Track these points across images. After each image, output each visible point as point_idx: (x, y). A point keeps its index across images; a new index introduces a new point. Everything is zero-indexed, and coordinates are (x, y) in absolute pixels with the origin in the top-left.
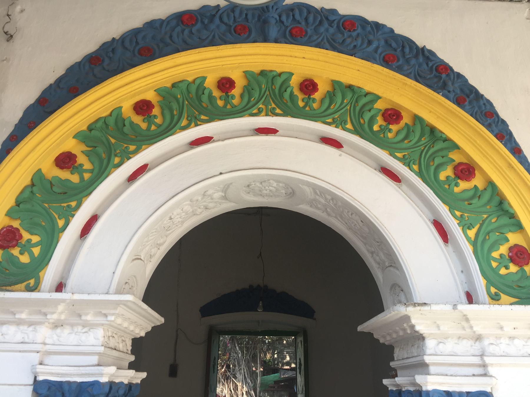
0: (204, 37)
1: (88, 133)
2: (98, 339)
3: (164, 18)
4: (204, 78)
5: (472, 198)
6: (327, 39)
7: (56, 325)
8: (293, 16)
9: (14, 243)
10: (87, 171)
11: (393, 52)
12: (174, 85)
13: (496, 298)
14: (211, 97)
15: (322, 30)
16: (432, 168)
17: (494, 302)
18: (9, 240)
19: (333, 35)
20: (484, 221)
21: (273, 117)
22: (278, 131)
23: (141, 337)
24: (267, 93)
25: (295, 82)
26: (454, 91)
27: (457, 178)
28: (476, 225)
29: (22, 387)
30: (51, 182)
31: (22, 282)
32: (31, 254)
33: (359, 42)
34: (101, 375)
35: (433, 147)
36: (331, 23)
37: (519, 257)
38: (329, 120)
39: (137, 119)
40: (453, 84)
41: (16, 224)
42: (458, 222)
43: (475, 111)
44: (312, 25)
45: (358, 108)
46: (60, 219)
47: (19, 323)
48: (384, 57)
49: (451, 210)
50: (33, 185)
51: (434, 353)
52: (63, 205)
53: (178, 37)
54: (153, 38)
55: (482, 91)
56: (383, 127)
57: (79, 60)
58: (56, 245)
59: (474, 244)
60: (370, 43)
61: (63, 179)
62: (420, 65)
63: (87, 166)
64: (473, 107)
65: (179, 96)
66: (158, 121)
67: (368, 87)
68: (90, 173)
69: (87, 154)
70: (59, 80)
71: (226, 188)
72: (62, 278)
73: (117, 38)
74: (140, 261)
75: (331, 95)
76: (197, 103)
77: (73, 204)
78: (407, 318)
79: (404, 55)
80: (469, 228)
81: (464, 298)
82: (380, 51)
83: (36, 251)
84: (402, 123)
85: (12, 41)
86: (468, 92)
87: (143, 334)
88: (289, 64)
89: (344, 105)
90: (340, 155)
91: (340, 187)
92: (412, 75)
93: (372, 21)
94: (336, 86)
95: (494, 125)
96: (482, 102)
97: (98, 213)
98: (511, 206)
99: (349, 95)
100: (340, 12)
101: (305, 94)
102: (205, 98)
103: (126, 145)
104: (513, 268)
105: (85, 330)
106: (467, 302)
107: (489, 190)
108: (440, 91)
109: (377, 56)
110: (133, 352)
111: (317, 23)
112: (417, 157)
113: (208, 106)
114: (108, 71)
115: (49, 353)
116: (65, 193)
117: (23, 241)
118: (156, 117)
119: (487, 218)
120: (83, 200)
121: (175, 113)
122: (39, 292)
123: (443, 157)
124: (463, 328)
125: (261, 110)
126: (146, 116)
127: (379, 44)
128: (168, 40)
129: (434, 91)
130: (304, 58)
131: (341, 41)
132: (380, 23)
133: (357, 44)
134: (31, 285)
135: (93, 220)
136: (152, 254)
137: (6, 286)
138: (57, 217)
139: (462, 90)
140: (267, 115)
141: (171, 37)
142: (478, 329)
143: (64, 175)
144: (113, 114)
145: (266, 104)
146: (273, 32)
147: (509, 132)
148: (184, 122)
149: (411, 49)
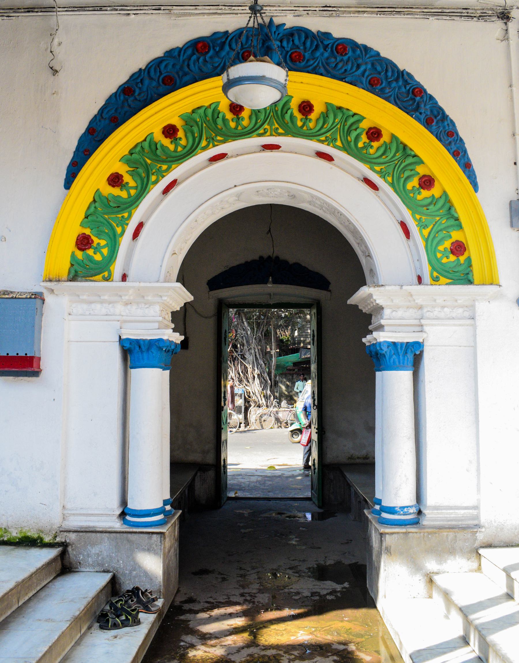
0: (216, 65)
1: (129, 157)
2: (156, 312)
3: (181, 46)
4: (218, 103)
5: (430, 204)
6: (322, 63)
7: (127, 304)
8: (293, 41)
9: (89, 245)
10: (132, 188)
11: (377, 76)
12: (193, 111)
13: (437, 279)
14: (224, 120)
15: (318, 54)
16: (402, 180)
17: (435, 283)
18: (85, 244)
19: (327, 59)
20: (436, 222)
21: (276, 136)
22: (280, 147)
24: (271, 114)
26: (425, 112)
27: (420, 188)
28: (429, 226)
29: (112, 343)
30: (107, 199)
31: (99, 274)
32: (102, 254)
33: (349, 66)
34: (164, 334)
35: (405, 162)
36: (326, 47)
37: (457, 250)
39: (166, 142)
40: (425, 105)
41: (88, 232)
42: (417, 223)
43: (440, 130)
44: (310, 48)
45: (346, 127)
46: (118, 227)
47: (102, 302)
48: (370, 80)
49: (413, 214)
50: (94, 201)
51: (389, 318)
52: (118, 216)
53: (194, 64)
54: (174, 65)
55: (448, 112)
56: (366, 144)
57: (114, 91)
58: (119, 247)
59: (427, 241)
60: (358, 67)
61: (116, 195)
62: (399, 88)
63: (132, 184)
64: (439, 126)
65: (198, 120)
66: (183, 142)
67: (354, 110)
68: (135, 189)
69: (131, 174)
70: (102, 111)
71: (239, 196)
72: (124, 270)
73: (143, 68)
75: (325, 116)
76: (213, 125)
77: (126, 215)
78: (370, 296)
79: (387, 78)
80: (424, 228)
81: (416, 280)
82: (367, 73)
83: (105, 251)
84: (382, 140)
85: (57, 74)
86: (436, 113)
89: (335, 124)
90: (331, 168)
92: (392, 98)
93: (361, 44)
94: (329, 108)
95: (453, 144)
96: (446, 123)
98: (456, 212)
99: (340, 116)
100: (333, 36)
101: (303, 115)
102: (220, 121)
103: (159, 165)
104: (452, 258)
105: (147, 306)
106: (417, 283)
107: (444, 198)
108: (412, 113)
109: (364, 80)
111: (314, 47)
112: (391, 171)
113: (222, 129)
114: (140, 101)
115: (125, 322)
116: (118, 207)
117: (95, 244)
118: (181, 140)
119: (439, 219)
120: (133, 211)
121: (196, 135)
122: (112, 281)
123: (412, 170)
124: (410, 301)
125: (266, 130)
126: (173, 139)
127: (366, 68)
128: (186, 69)
129: (408, 113)
130: (302, 83)
131: (334, 65)
132: (369, 46)
133: (348, 68)
134: (106, 276)
135: (141, 225)
139: (432, 111)
140: (271, 135)
141: (188, 65)
142: (419, 301)
143: (116, 191)
144: (147, 140)
145: (271, 124)
147: (464, 149)
148: (204, 143)
149: (393, 71)
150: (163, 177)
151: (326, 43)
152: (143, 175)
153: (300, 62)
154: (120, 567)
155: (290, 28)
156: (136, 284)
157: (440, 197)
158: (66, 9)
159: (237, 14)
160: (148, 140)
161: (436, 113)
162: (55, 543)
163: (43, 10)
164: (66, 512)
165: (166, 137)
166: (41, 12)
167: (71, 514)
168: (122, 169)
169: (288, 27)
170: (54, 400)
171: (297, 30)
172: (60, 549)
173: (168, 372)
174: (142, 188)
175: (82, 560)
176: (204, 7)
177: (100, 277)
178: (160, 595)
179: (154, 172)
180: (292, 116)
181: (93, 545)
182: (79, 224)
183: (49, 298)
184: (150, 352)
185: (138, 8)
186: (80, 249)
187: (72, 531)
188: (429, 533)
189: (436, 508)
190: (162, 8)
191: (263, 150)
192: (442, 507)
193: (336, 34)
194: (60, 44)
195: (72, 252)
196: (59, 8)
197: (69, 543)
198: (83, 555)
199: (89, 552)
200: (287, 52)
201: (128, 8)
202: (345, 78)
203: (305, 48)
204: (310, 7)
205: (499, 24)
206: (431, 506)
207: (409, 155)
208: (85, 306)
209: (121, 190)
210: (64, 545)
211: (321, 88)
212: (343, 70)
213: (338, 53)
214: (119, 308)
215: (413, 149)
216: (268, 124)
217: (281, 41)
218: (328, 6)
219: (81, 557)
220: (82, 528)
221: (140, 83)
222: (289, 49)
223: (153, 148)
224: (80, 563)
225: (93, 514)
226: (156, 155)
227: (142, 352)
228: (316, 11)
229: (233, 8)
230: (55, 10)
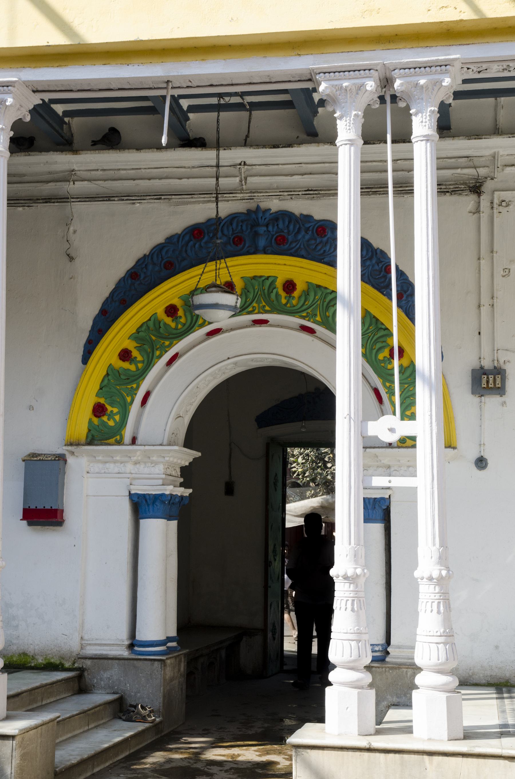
3: (180, 233)
7: (136, 463)
8: (277, 225)
9: (104, 412)
10: (139, 362)
13: (404, 441)
15: (300, 236)
16: (374, 351)
17: (402, 445)
23: (186, 466)
24: (259, 293)
25: (279, 284)
29: (124, 497)
31: (112, 438)
32: (114, 420)
34: (166, 490)
35: (377, 334)
38: (304, 314)
39: (168, 320)
41: (102, 401)
43: (409, 304)
45: (325, 304)
47: (115, 462)
50: (107, 374)
52: (128, 387)
54: (174, 251)
58: (129, 414)
61: (126, 368)
62: (373, 266)
63: (139, 358)
64: (409, 301)
66: (183, 320)
70: (112, 293)
72: (134, 433)
73: (147, 254)
74: (180, 418)
75: (306, 294)
77: (135, 386)
83: (117, 418)
87: (187, 464)
88: (273, 269)
89: (316, 301)
90: (313, 341)
91: (311, 366)
97: (150, 389)
99: (319, 294)
100: (315, 218)
101: (287, 293)
103: (162, 342)
105: (153, 465)
107: (411, 367)
108: (383, 290)
110: (182, 476)
115: (135, 479)
116: (128, 379)
119: (407, 387)
120: (140, 383)
124: (377, 461)
125: (254, 308)
128: (184, 255)
131: (314, 247)
134: (118, 440)
135: (147, 395)
136: (188, 410)
137: (104, 440)
138: (126, 395)
140: (259, 313)
141: (186, 251)
142: (386, 461)
143: (126, 365)
145: (259, 302)
146: (262, 242)
150: (166, 352)
151: (307, 225)
152: (149, 350)
153: (283, 245)
154: (127, 690)
155: (276, 212)
156: (142, 448)
157: (409, 367)
158: (79, 200)
159: (228, 201)
160: (152, 319)
161: (405, 289)
162: (74, 668)
163: (59, 200)
164: (83, 642)
165: (168, 316)
166: (57, 202)
167: (86, 644)
168: (130, 345)
169: (274, 212)
170: (75, 546)
171: (282, 214)
172: (78, 672)
173: (174, 524)
174: (148, 361)
175: (96, 683)
176: (199, 196)
177: (112, 440)
178: (160, 715)
179: (158, 348)
180: (277, 295)
181: (105, 670)
182: (95, 395)
183: (70, 460)
184: (155, 506)
185: (142, 198)
186: (96, 416)
187: (88, 658)
188: (392, 668)
189: (399, 647)
190: (163, 197)
191: (254, 325)
192: (403, 646)
193: (317, 217)
194: (75, 232)
195: (89, 419)
196: (73, 198)
197: (85, 668)
198: (97, 680)
199: (102, 676)
200: (273, 235)
201: (133, 198)
202: (323, 259)
203: (289, 231)
204: (294, 191)
205: (473, 197)
206: (394, 645)
207: (381, 328)
208: (101, 466)
209: (130, 364)
210: (81, 671)
211: (302, 269)
212: (322, 251)
213: (318, 235)
214: (129, 467)
215: (384, 323)
216: (256, 303)
217: (267, 226)
218: (310, 189)
219: (95, 681)
220: (96, 655)
221: (144, 269)
222: (274, 233)
223: (157, 327)
224: (94, 686)
225: (106, 644)
226: (160, 333)
227: (148, 505)
228: (299, 195)
229: (225, 195)
230: (69, 200)
